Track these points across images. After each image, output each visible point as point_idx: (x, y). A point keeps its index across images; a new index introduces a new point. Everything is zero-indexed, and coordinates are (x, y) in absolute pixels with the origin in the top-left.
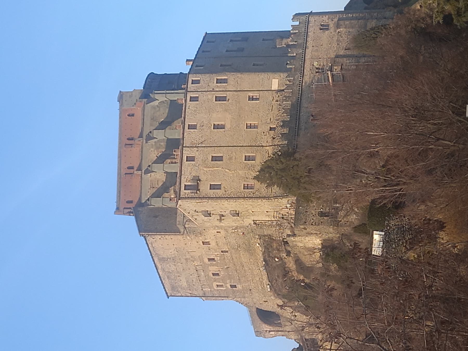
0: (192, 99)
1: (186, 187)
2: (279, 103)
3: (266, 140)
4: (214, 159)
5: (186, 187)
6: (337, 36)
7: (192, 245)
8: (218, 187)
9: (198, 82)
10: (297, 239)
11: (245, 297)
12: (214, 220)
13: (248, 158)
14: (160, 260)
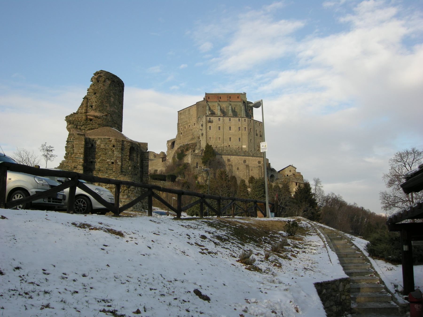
3: (226, 144)
4: (219, 127)
7: (194, 120)
9: (245, 121)
12: (201, 127)
13: (219, 138)
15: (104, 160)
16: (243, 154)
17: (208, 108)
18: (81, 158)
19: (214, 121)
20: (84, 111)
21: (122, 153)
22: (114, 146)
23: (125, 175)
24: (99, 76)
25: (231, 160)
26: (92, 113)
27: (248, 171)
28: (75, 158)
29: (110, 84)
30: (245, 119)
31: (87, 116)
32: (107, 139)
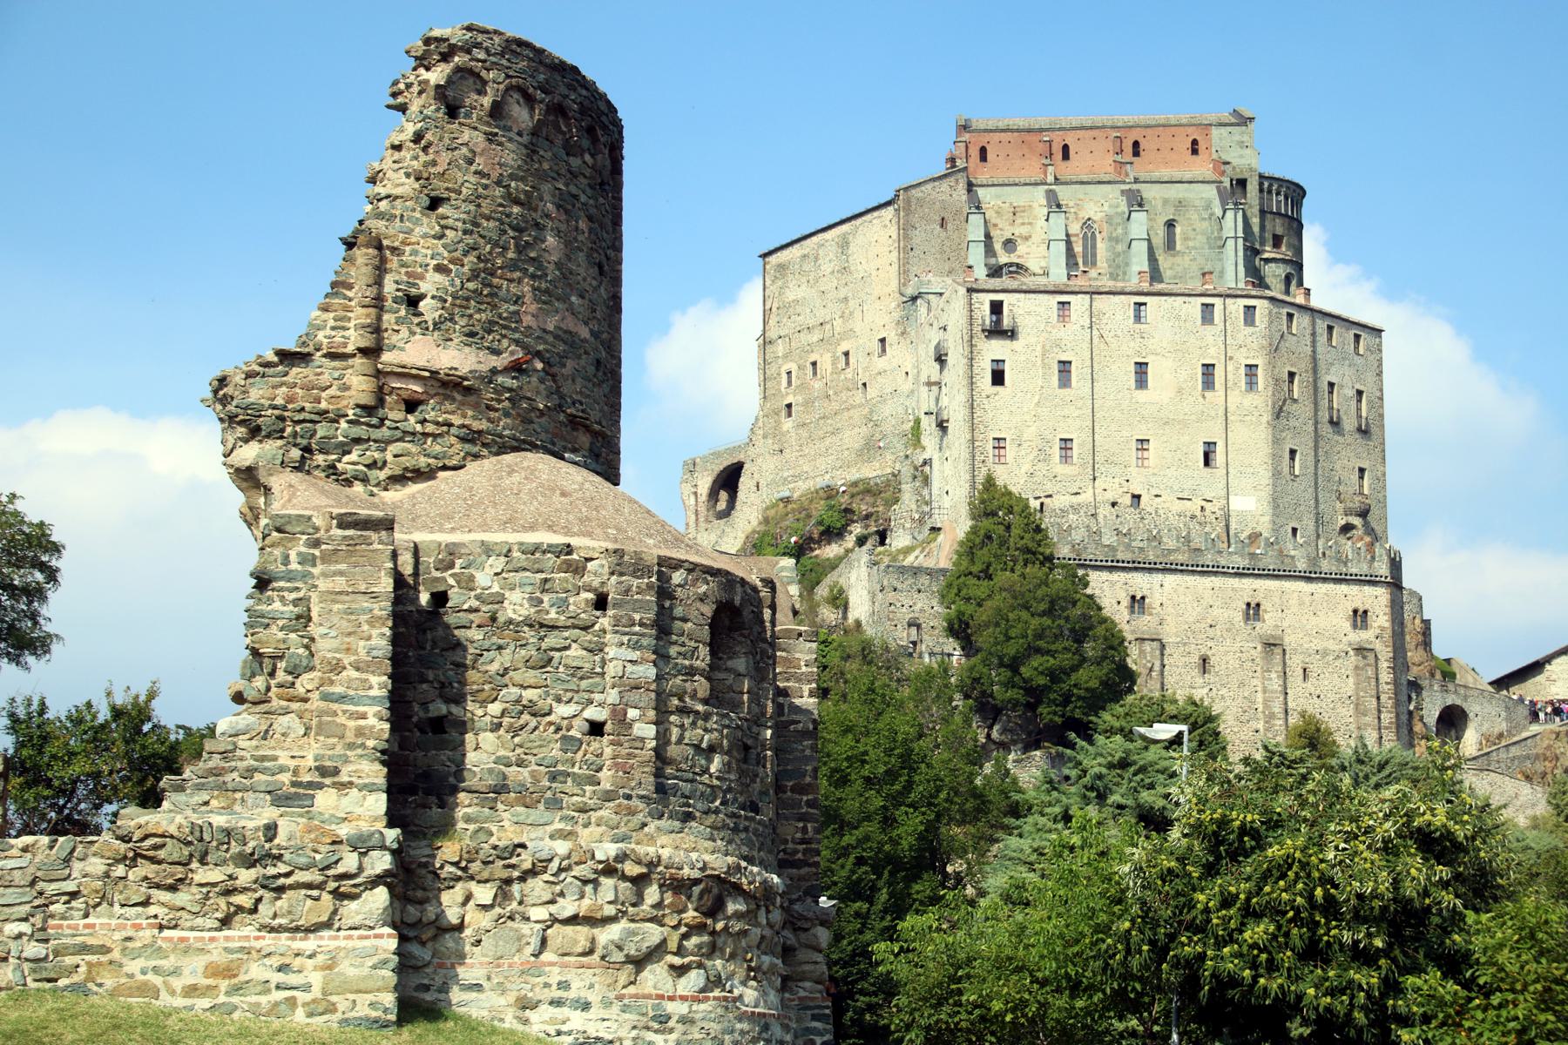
0: (1208, 307)
1: (997, 308)
2: (1198, 513)
3: (1112, 487)
4: (1065, 367)
5: (997, 308)
6: (1336, 648)
7: (880, 315)
8: (998, 378)
10: (864, 570)
11: (765, 437)
13: (1066, 444)
14: (844, 236)
15: (532, 710)
16: (1241, 562)
17: (975, 230)
18: (374, 700)
19: (1026, 326)
20: (354, 339)
21: (661, 656)
22: (601, 603)
23: (687, 817)
24: (458, 69)
25: (1153, 601)
26: (415, 350)
27: (1275, 684)
28: (326, 697)
29: (535, 132)
30: (1250, 309)
31: (378, 374)
32: (550, 549)
